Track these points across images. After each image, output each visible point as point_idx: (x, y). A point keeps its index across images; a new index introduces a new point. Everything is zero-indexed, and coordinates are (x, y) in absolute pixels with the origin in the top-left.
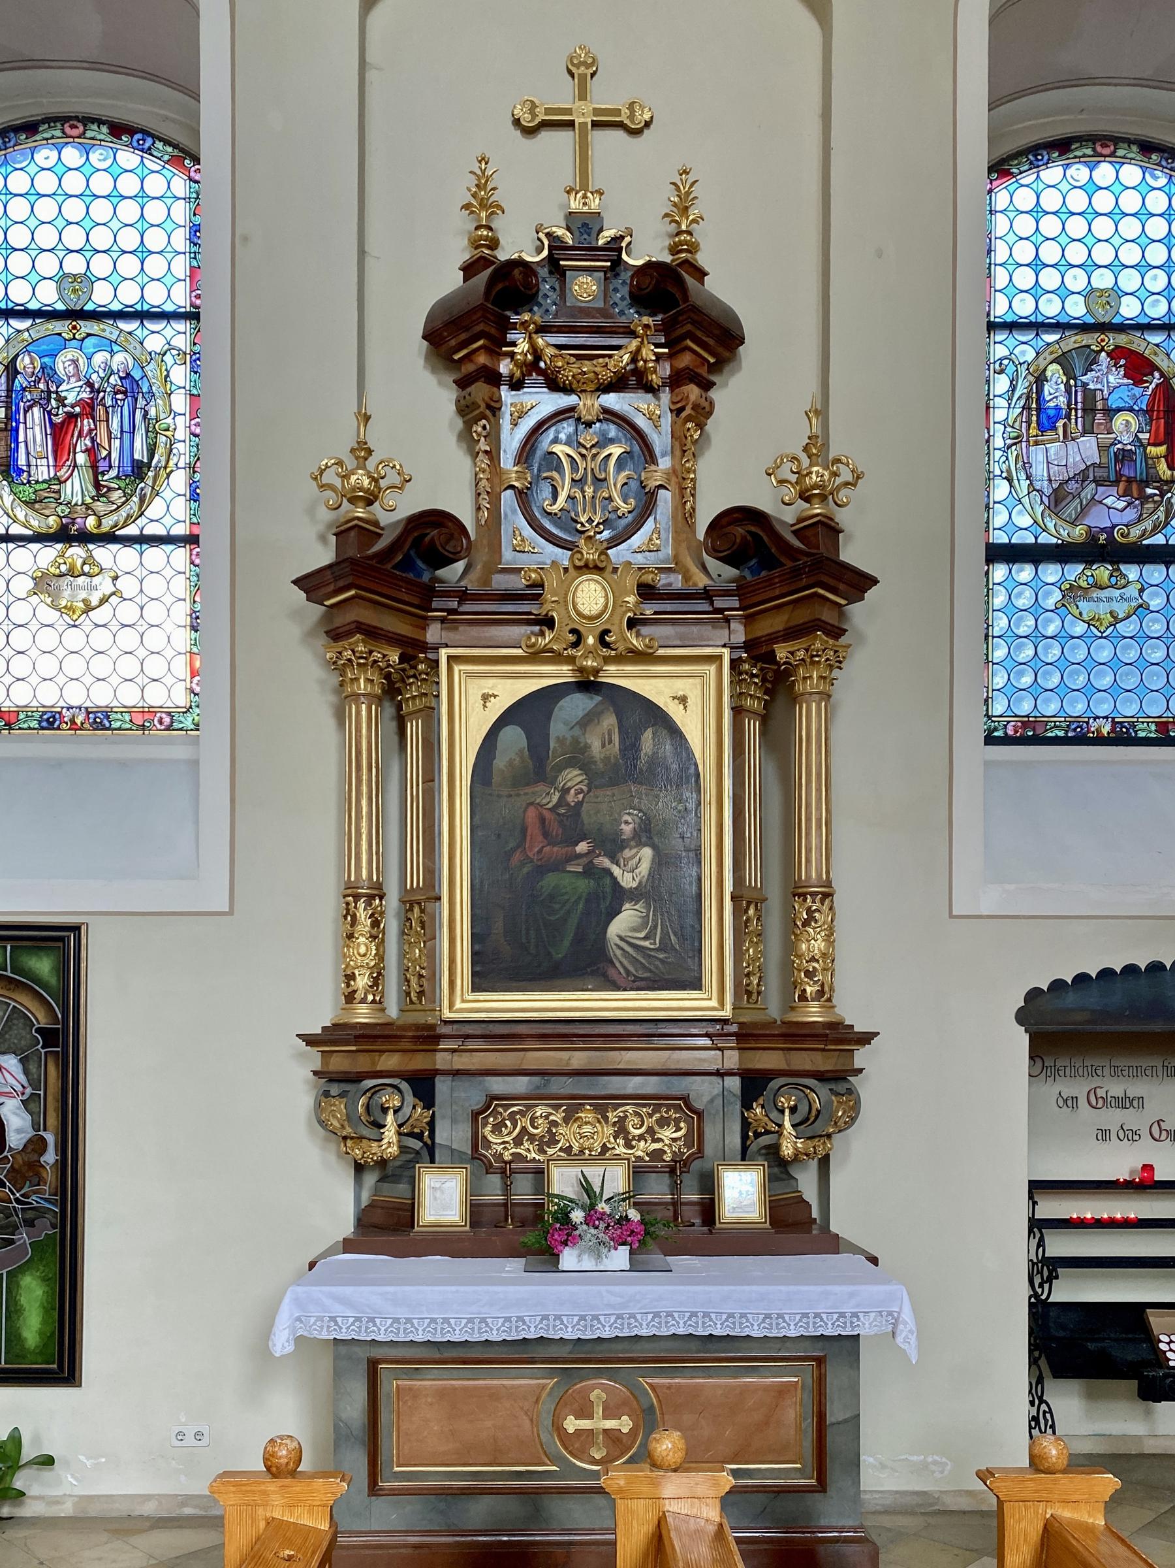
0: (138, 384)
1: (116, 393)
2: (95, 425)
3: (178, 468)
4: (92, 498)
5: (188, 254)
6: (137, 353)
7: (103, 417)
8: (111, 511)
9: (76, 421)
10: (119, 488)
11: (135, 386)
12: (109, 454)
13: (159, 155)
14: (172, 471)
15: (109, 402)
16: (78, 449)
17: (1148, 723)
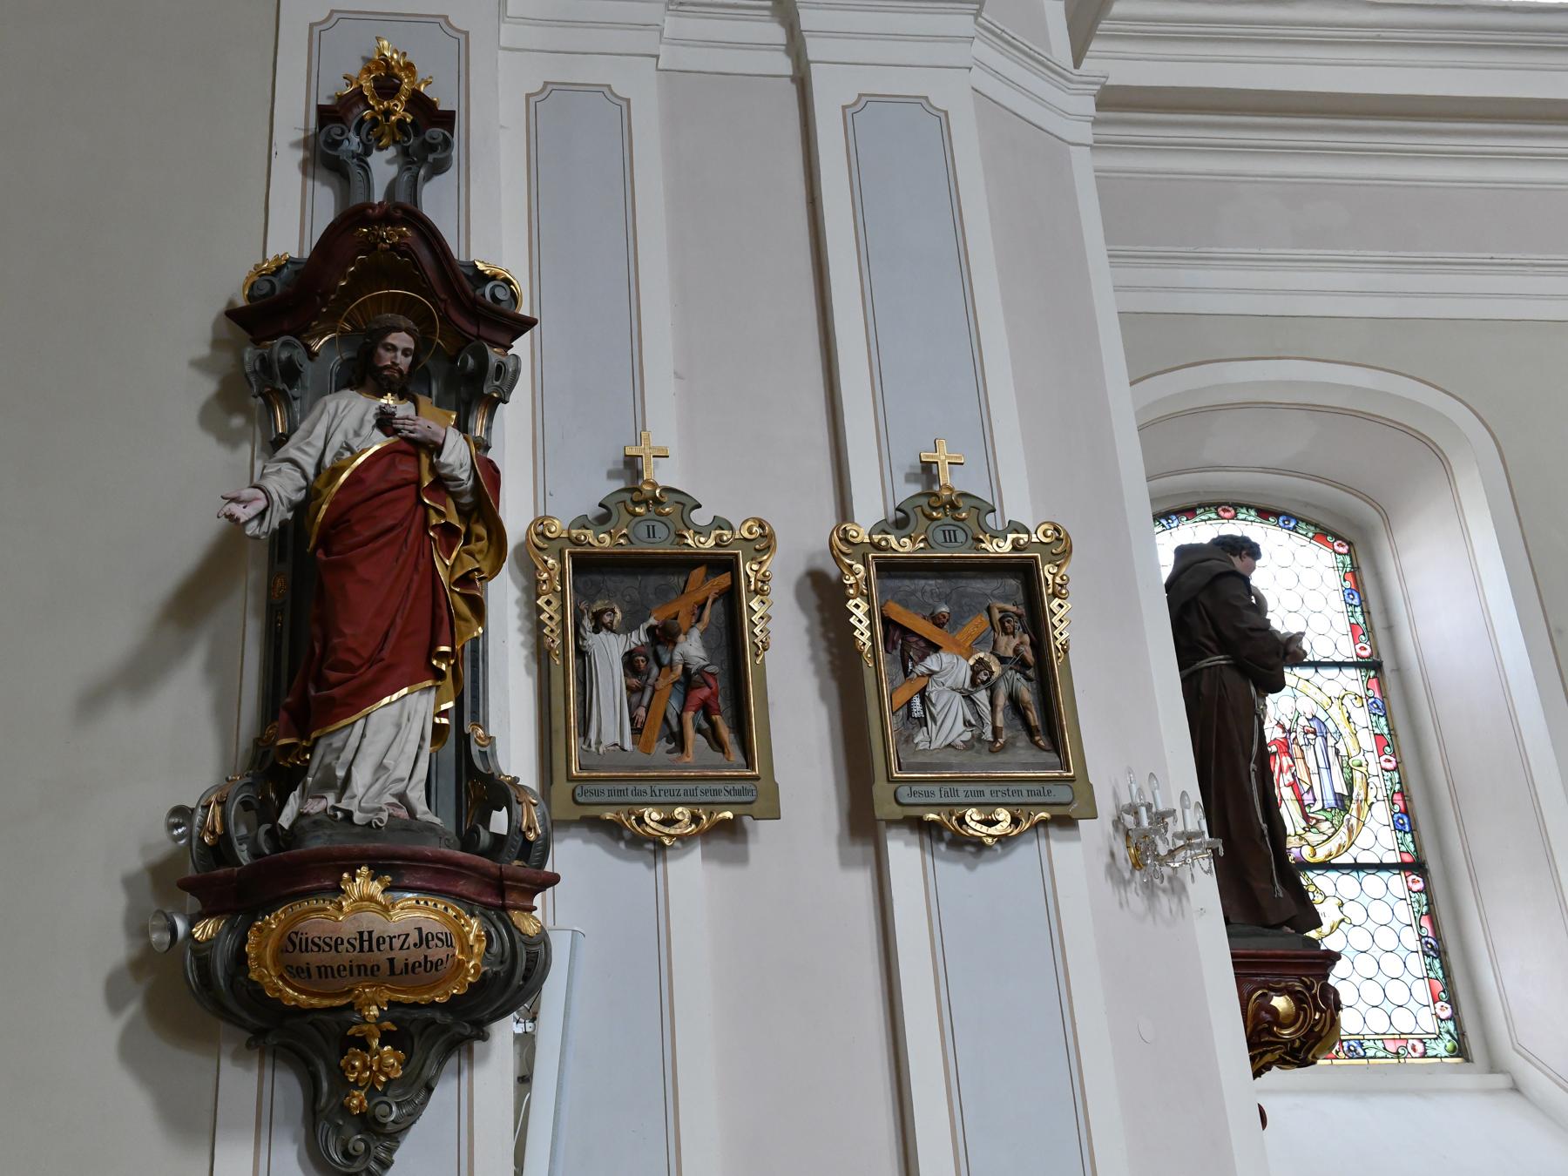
0: (1325, 726)
1: (1306, 734)
2: (1294, 762)
3: (1378, 801)
4: (1304, 829)
5: (1346, 613)
6: (1318, 699)
7: (1299, 755)
8: (1324, 841)
9: (1275, 759)
10: (1327, 820)
11: (1323, 727)
12: (1311, 787)
13: (1304, 533)
14: (1372, 803)
15: (1301, 741)
16: (1282, 785)
17: (1374, 1040)
